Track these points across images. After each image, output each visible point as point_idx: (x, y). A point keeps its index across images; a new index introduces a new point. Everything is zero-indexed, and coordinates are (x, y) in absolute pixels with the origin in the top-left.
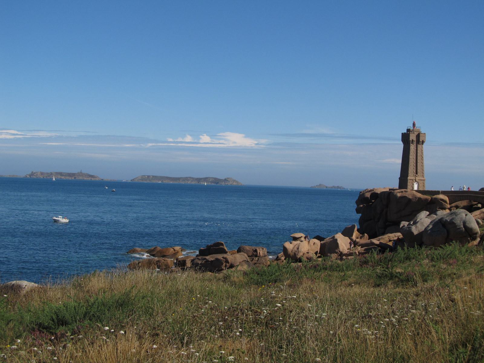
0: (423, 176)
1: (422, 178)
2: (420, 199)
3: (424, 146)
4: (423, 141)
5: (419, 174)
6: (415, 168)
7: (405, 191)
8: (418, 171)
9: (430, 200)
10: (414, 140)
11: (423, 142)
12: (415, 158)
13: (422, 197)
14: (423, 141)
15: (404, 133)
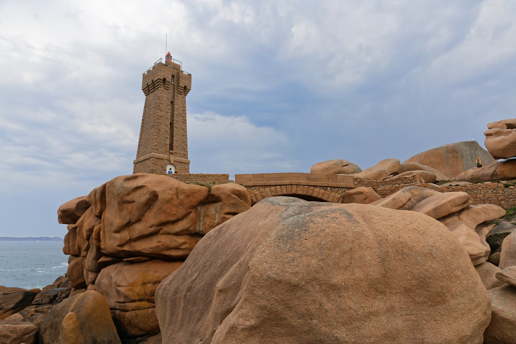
0: (185, 156)
1: (183, 160)
2: (178, 192)
3: (189, 97)
4: (185, 87)
5: (175, 150)
6: (169, 136)
7: (142, 176)
8: (175, 144)
9: (206, 193)
10: (167, 80)
11: (186, 90)
12: (169, 116)
13: (186, 188)
14: (185, 87)
15: (149, 71)
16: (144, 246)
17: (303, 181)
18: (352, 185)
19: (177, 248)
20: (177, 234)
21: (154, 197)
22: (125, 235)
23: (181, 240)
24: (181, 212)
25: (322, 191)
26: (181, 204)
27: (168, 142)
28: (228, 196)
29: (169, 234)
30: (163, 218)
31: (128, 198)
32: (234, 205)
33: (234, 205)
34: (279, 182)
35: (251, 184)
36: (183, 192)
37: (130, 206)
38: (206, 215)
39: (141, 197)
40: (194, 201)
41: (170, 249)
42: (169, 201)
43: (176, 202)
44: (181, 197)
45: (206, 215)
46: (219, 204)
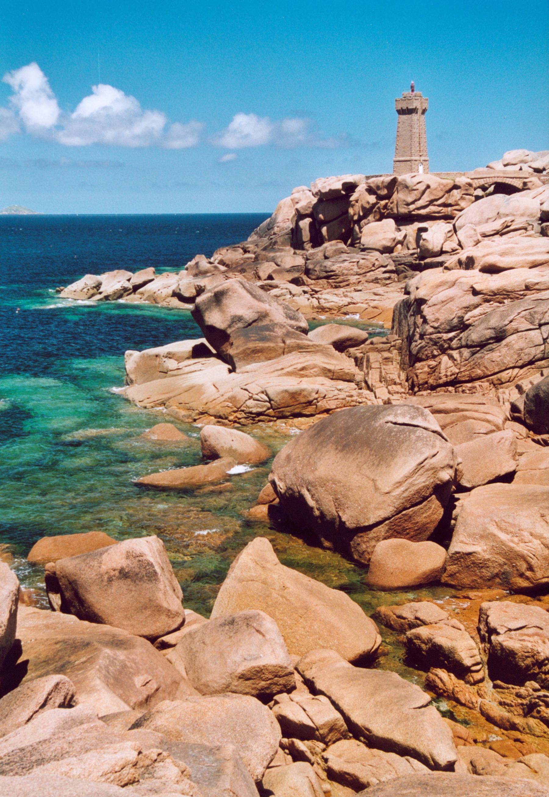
2: (440, 184)
16: (423, 212)
17: (502, 175)
18: (527, 176)
19: (439, 212)
20: (439, 206)
21: (428, 187)
22: (412, 207)
23: (441, 208)
24: (441, 194)
25: (511, 180)
26: (442, 190)
27: (418, 149)
28: (464, 186)
29: (435, 205)
30: (433, 197)
31: (415, 188)
32: (467, 190)
33: (467, 190)
34: (488, 176)
35: (473, 177)
36: (442, 184)
37: (415, 192)
38: (453, 196)
39: (422, 187)
40: (448, 188)
41: (434, 212)
42: (435, 189)
43: (439, 189)
44: (442, 187)
45: (453, 196)
46: (459, 190)
